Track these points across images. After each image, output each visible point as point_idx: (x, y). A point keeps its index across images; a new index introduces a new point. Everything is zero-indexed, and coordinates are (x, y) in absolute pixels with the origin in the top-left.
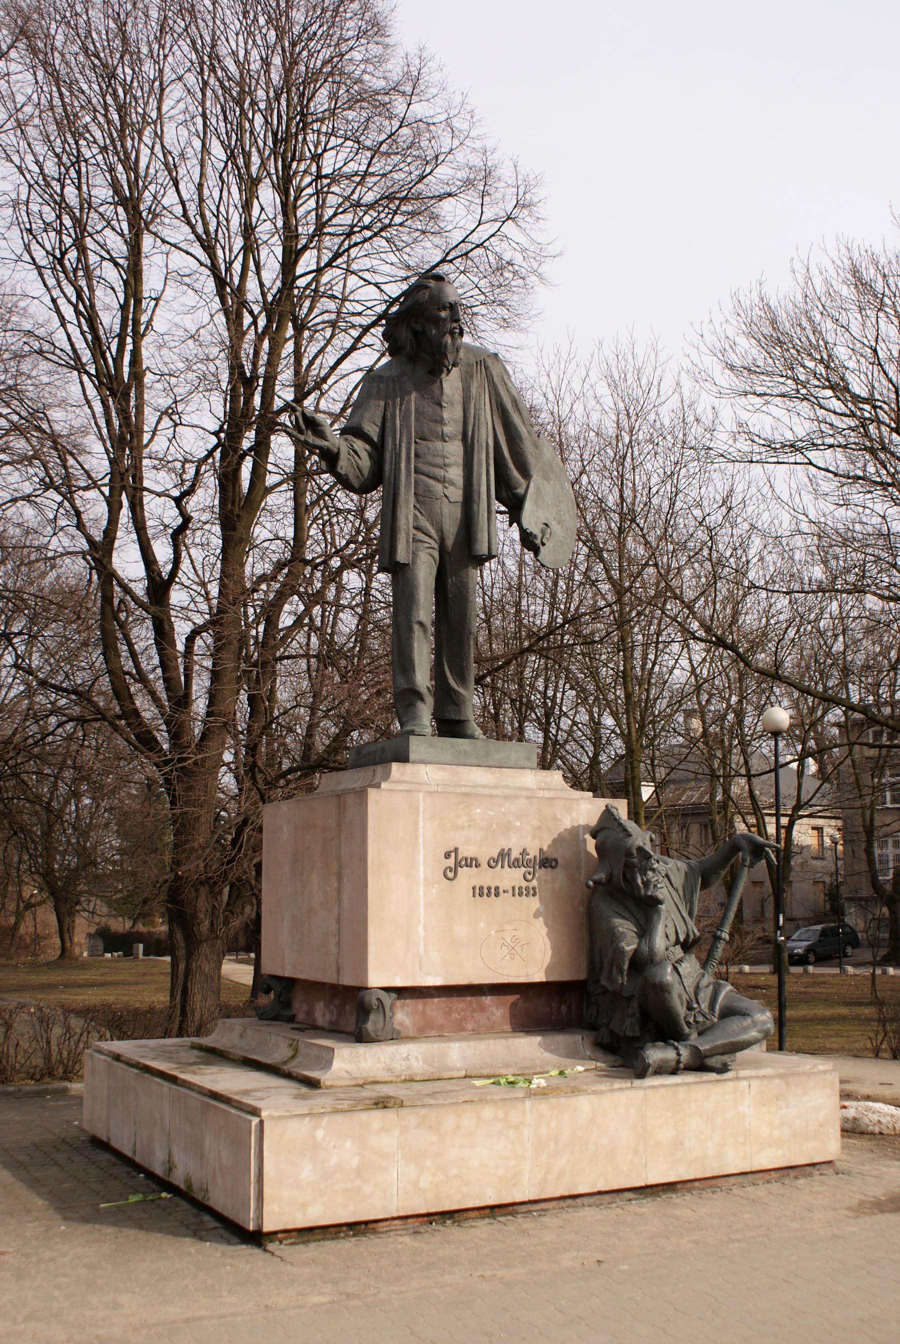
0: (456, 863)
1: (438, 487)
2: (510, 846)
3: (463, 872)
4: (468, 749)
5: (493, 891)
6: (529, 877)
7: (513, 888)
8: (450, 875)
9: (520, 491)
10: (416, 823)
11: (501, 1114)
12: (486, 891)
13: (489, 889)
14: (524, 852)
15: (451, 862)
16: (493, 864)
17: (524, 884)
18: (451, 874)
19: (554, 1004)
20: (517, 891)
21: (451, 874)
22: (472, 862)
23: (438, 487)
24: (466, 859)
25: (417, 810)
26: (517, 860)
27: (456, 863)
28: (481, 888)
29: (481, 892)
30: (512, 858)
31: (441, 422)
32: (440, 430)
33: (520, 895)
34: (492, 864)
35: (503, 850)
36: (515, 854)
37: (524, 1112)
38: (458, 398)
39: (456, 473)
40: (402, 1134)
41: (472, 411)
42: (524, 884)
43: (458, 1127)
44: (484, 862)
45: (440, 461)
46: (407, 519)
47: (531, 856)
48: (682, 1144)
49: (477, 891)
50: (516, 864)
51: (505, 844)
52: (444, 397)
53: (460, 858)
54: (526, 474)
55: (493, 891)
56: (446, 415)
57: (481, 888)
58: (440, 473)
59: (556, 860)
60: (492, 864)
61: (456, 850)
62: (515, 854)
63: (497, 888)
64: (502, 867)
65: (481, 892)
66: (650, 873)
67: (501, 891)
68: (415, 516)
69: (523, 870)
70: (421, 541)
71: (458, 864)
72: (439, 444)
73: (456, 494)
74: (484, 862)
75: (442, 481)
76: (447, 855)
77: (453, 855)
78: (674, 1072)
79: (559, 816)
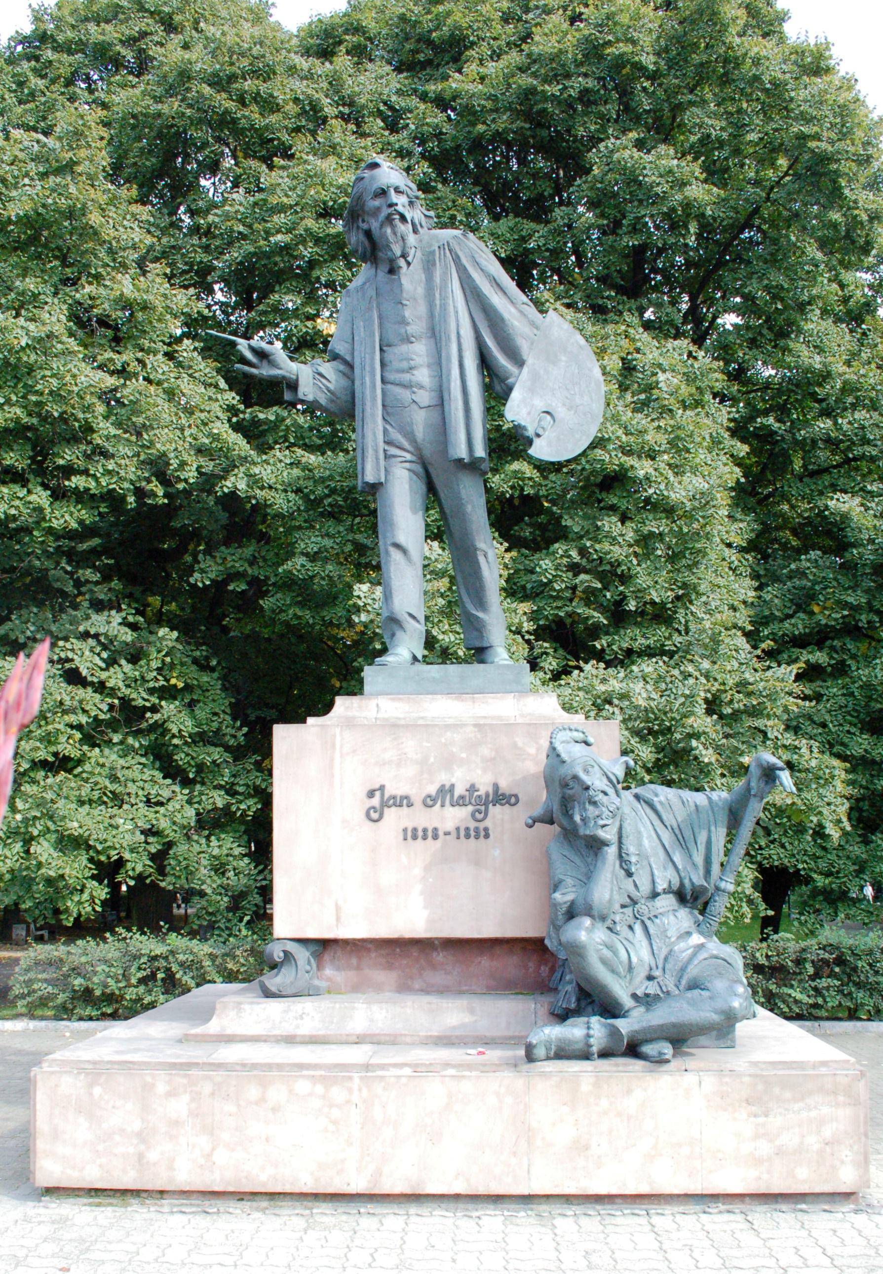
0: (381, 803)
1: (405, 395)
2: (453, 780)
3: (391, 814)
4: (436, 675)
5: (430, 834)
6: (479, 816)
7: (458, 829)
8: (375, 816)
9: (511, 380)
10: (332, 760)
11: (319, 1089)
12: (420, 833)
13: (425, 830)
14: (472, 789)
15: (376, 801)
16: (430, 803)
17: (472, 825)
18: (374, 816)
19: (531, 964)
20: (462, 833)
21: (374, 816)
22: (403, 801)
23: (405, 395)
24: (394, 797)
25: (333, 746)
26: (462, 797)
27: (381, 803)
28: (415, 830)
29: (413, 834)
30: (456, 795)
31: (403, 322)
32: (403, 331)
33: (468, 836)
34: (429, 802)
35: (443, 786)
36: (459, 791)
37: (350, 1091)
38: (420, 291)
39: (423, 376)
40: (193, 1100)
41: (438, 302)
42: (472, 825)
43: (262, 1100)
44: (417, 800)
45: (405, 365)
46: (374, 434)
47: (482, 792)
48: (587, 1148)
49: (409, 834)
50: (461, 802)
51: (444, 778)
52: (405, 295)
53: (386, 796)
54: (520, 363)
55: (430, 834)
56: (407, 313)
57: (415, 830)
58: (406, 377)
59: (516, 796)
60: (429, 802)
61: (382, 788)
62: (459, 791)
63: (435, 829)
64: (443, 806)
65: (413, 834)
66: (590, 808)
67: (441, 833)
68: (385, 431)
69: (470, 808)
70: (395, 456)
71: (384, 804)
72: (404, 348)
73: (425, 397)
74: (417, 800)
75: (408, 386)
76: (371, 794)
77: (378, 794)
78: (585, 1056)
79: (520, 744)
